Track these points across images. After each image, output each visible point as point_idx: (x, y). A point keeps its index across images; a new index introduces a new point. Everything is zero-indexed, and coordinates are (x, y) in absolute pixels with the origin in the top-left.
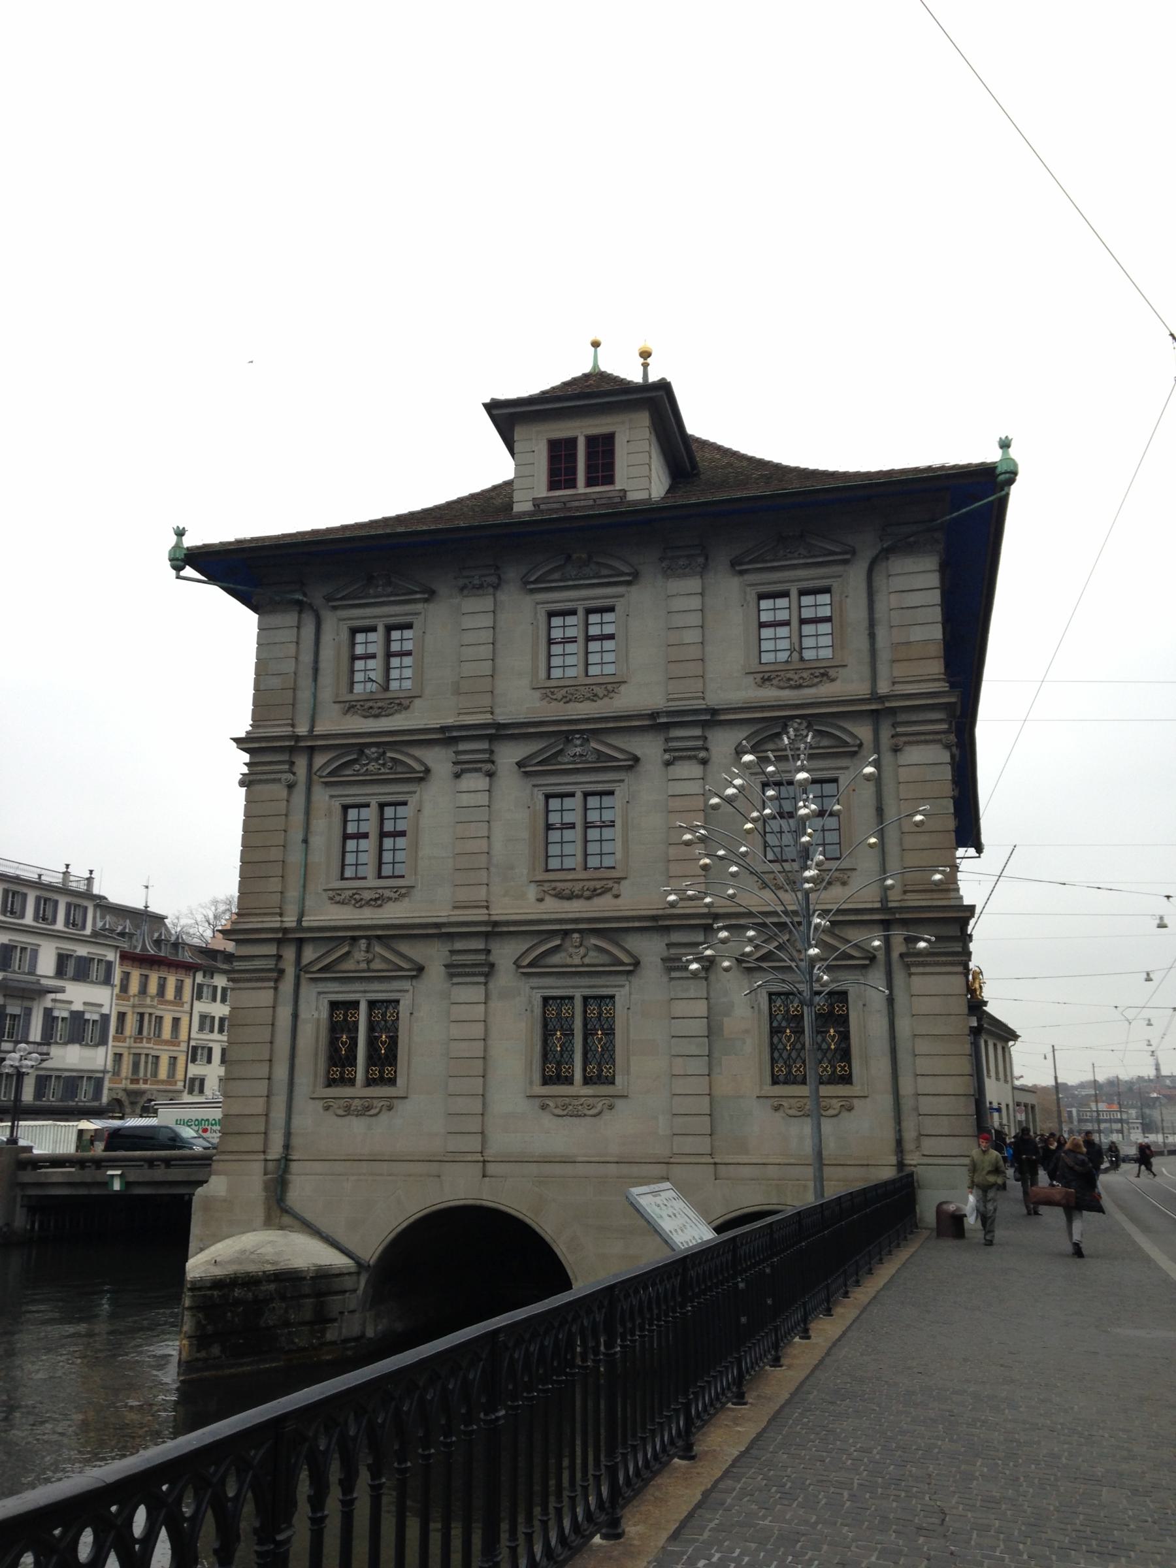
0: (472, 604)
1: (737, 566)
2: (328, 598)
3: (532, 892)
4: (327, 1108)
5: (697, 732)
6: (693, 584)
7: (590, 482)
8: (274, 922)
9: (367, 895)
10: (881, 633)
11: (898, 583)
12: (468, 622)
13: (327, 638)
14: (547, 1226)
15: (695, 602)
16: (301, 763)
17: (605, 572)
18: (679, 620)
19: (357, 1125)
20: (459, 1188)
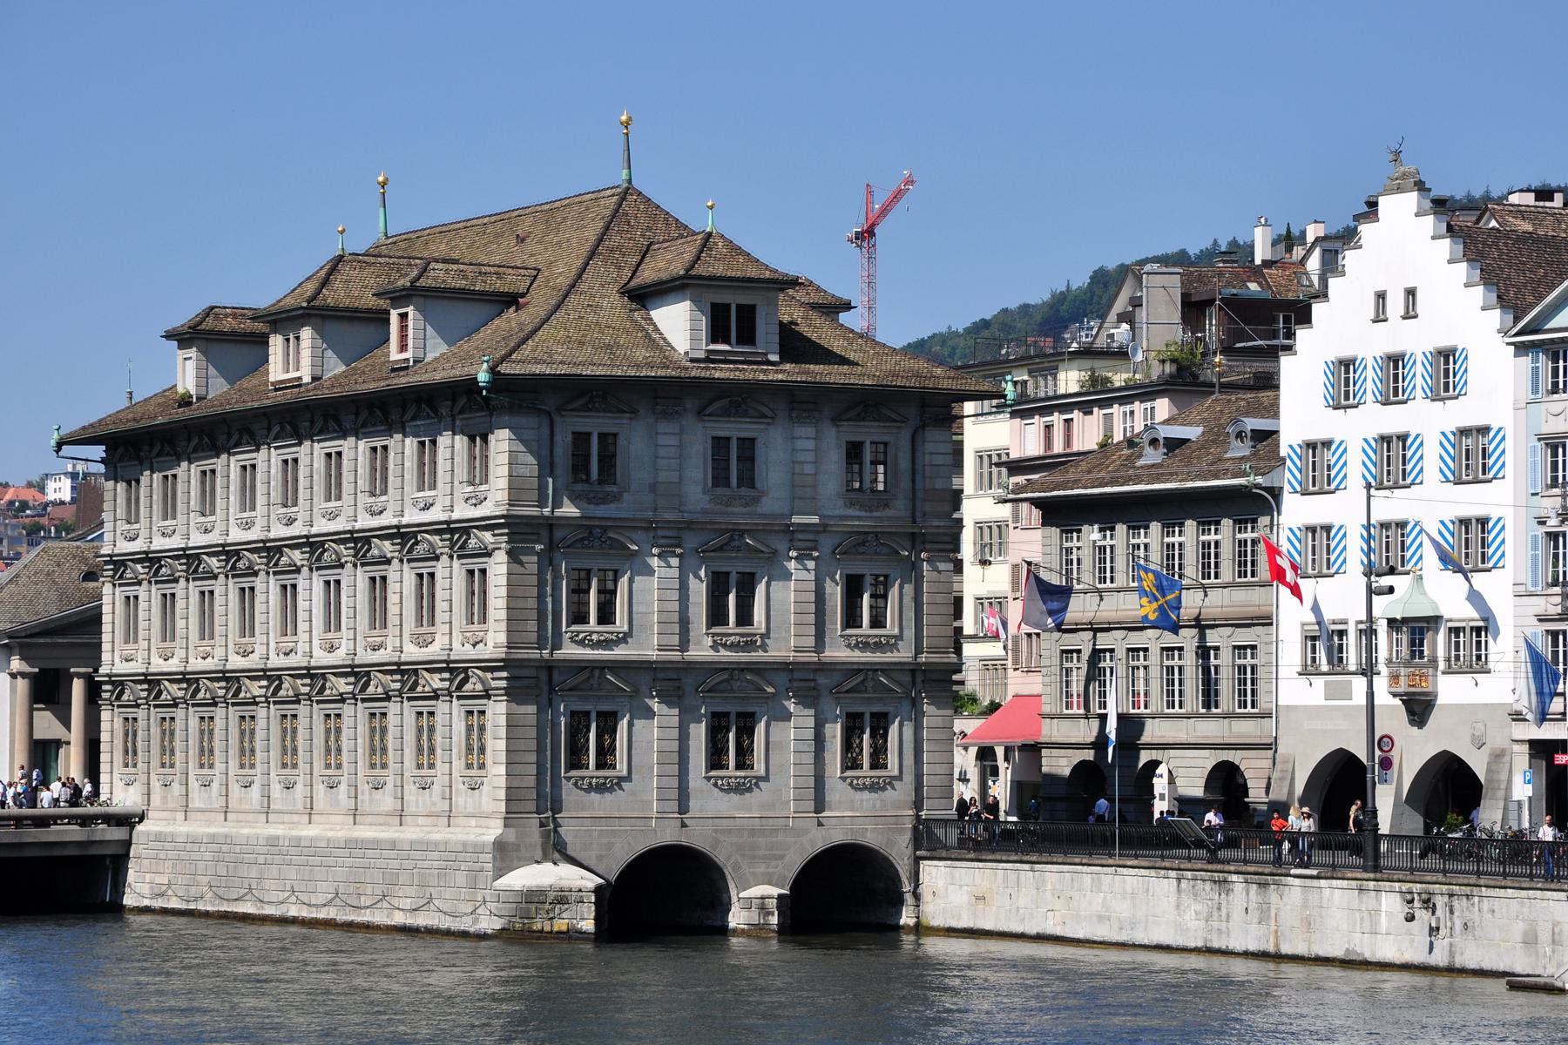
0: (663, 427)
1: (836, 419)
2: (559, 410)
3: (709, 641)
4: (576, 784)
5: (811, 537)
6: (810, 431)
7: (740, 342)
8: (534, 654)
9: (595, 637)
10: (918, 478)
11: (929, 447)
12: (662, 440)
13: (558, 438)
14: (720, 857)
15: (811, 444)
16: (545, 533)
17: (751, 412)
18: (801, 457)
19: (594, 796)
20: (668, 835)
